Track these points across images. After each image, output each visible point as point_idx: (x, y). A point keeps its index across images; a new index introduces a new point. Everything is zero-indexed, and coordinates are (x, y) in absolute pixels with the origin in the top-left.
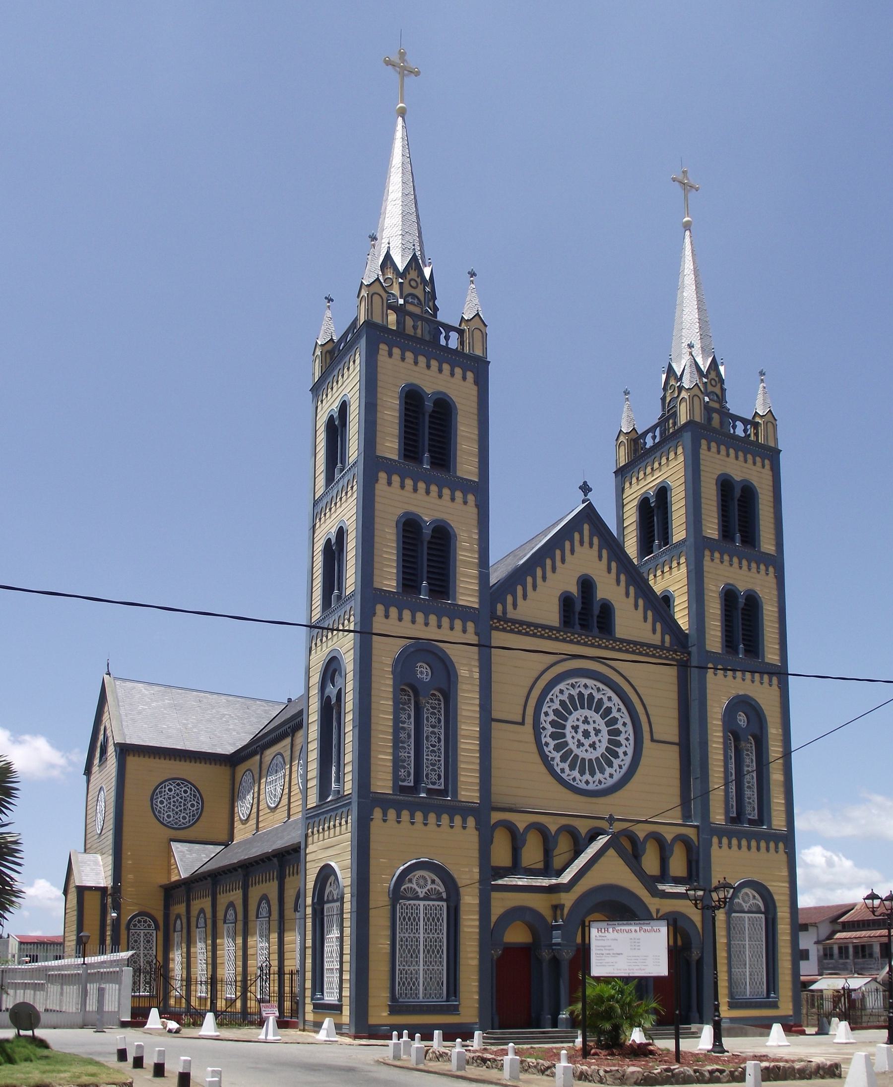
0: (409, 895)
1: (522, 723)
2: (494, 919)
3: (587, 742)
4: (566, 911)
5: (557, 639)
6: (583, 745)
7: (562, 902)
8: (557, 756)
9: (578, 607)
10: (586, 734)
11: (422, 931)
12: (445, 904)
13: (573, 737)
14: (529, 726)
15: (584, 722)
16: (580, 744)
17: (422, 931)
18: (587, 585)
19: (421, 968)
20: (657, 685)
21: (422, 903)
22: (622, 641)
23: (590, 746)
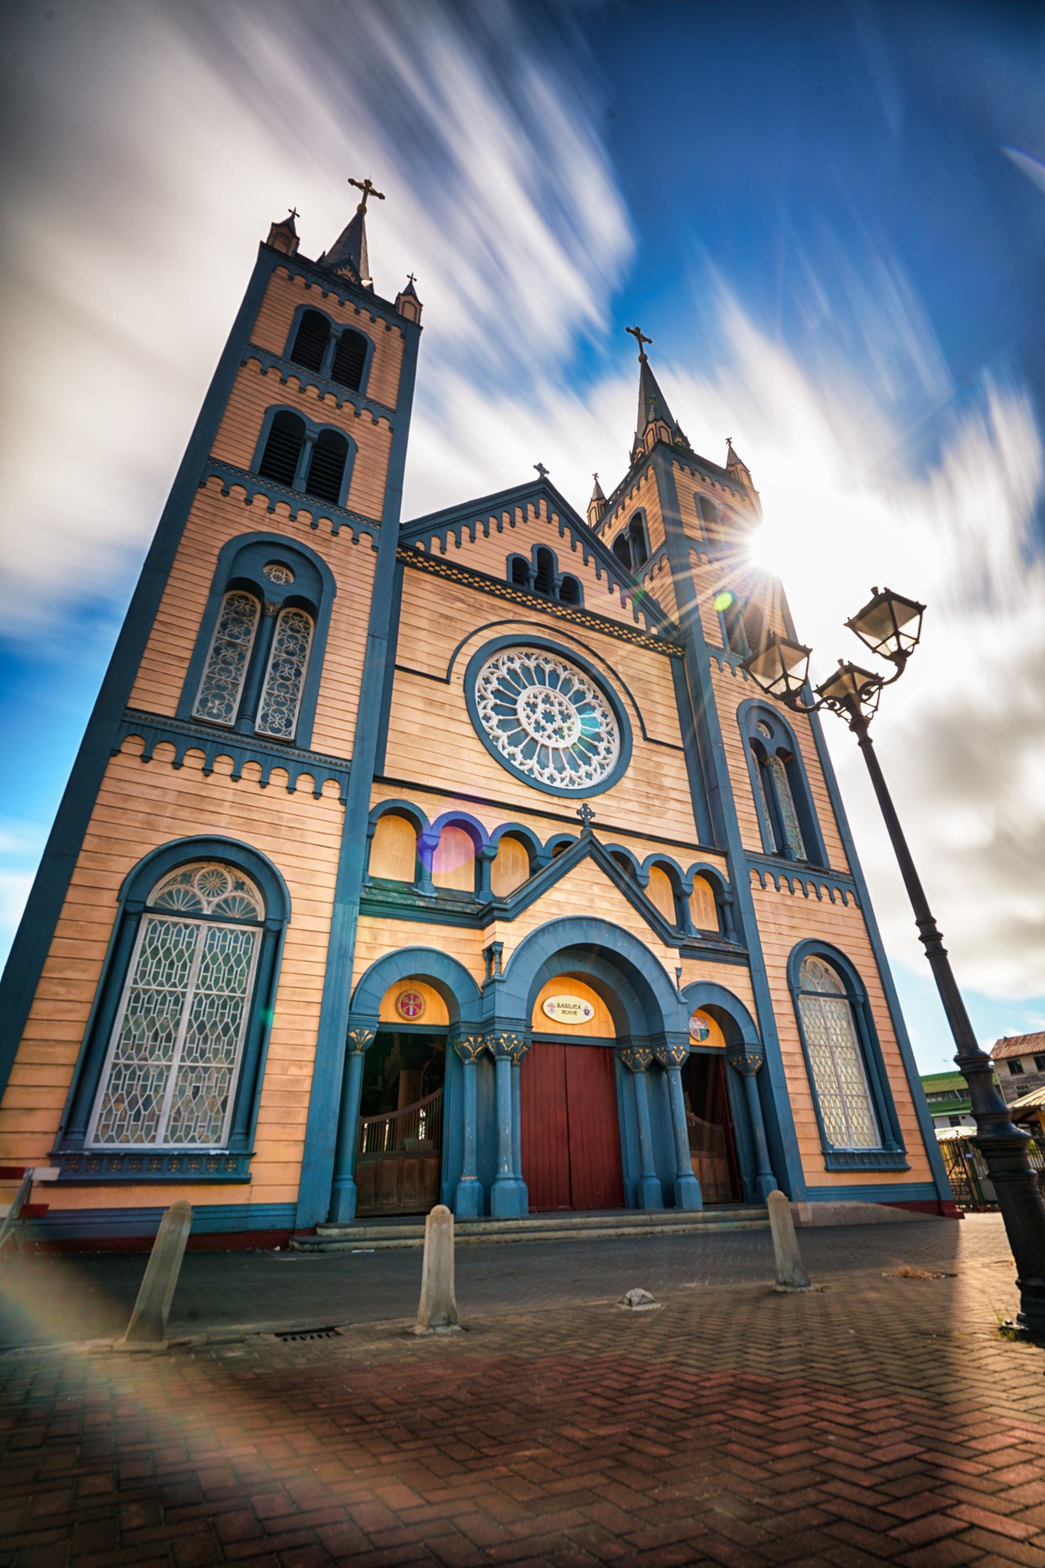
0: (179, 906)
1: (447, 681)
2: (361, 967)
3: (550, 727)
4: (506, 956)
5: (502, 597)
6: (544, 729)
7: (499, 938)
8: (504, 736)
9: (534, 570)
10: (549, 717)
11: (193, 981)
12: (259, 931)
13: (528, 717)
14: (456, 688)
15: (543, 701)
16: (538, 727)
17: (193, 981)
18: (544, 555)
19: (176, 1062)
20: (643, 672)
21: (205, 925)
22: (595, 616)
23: (555, 732)
